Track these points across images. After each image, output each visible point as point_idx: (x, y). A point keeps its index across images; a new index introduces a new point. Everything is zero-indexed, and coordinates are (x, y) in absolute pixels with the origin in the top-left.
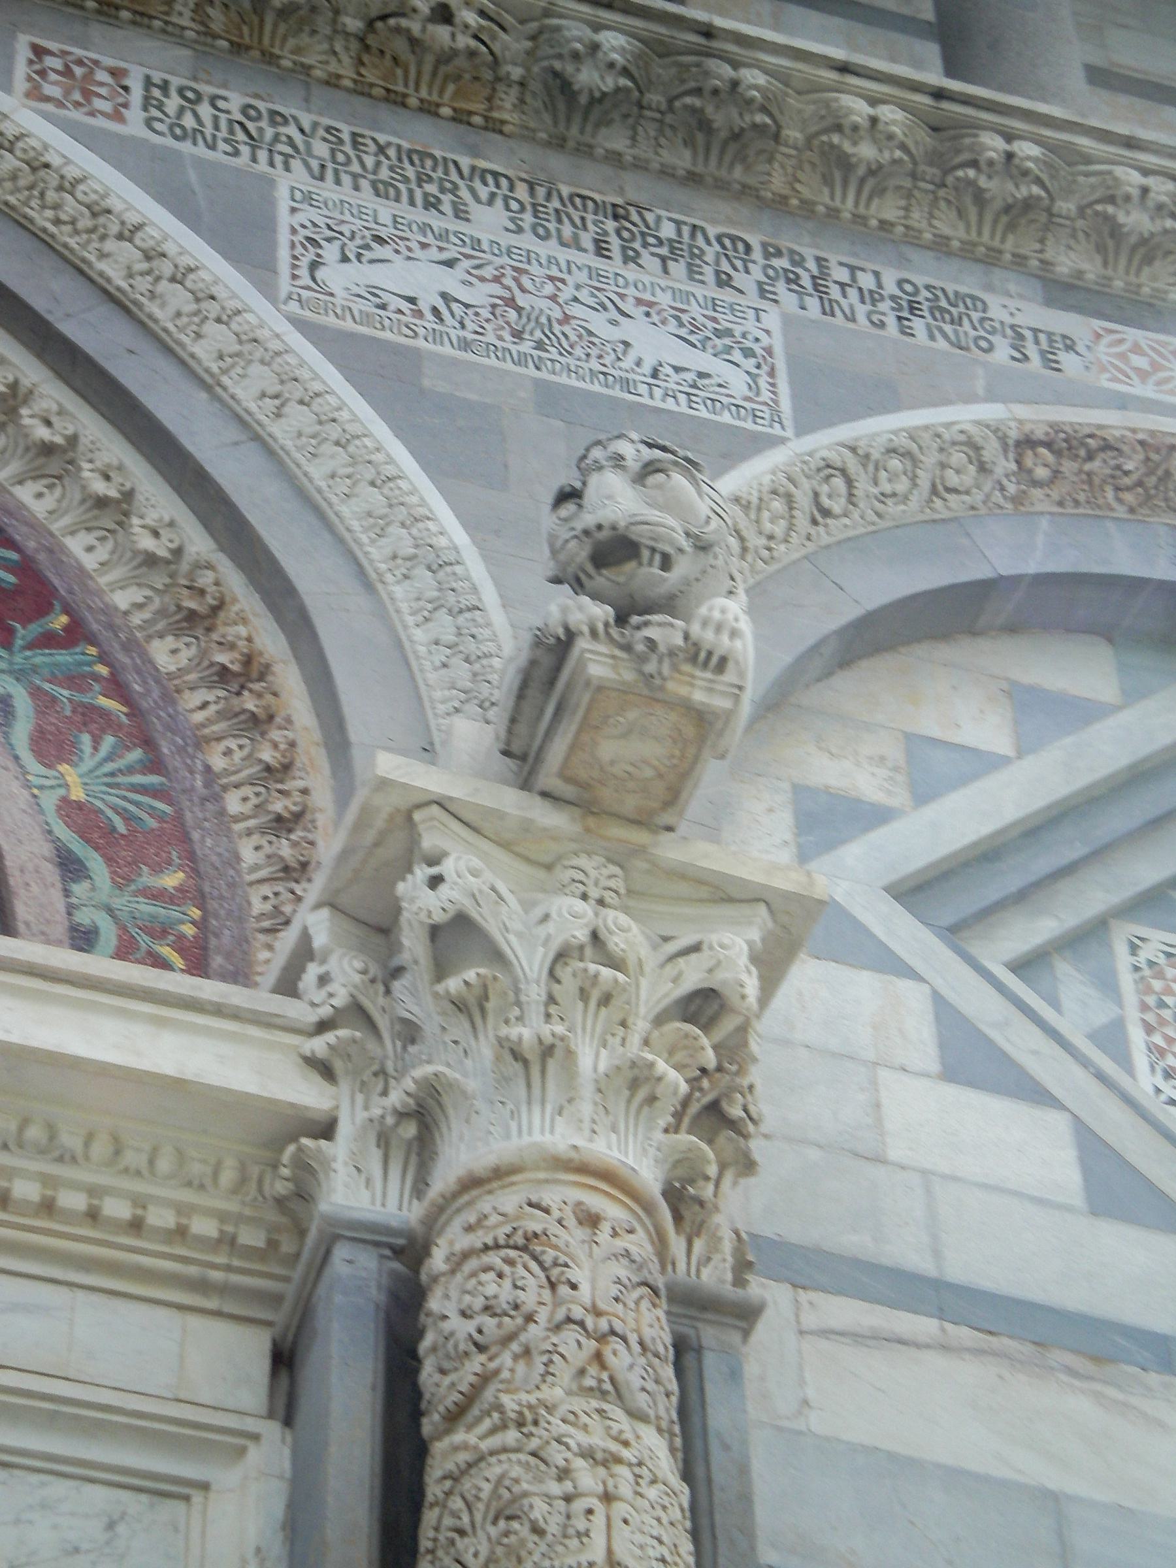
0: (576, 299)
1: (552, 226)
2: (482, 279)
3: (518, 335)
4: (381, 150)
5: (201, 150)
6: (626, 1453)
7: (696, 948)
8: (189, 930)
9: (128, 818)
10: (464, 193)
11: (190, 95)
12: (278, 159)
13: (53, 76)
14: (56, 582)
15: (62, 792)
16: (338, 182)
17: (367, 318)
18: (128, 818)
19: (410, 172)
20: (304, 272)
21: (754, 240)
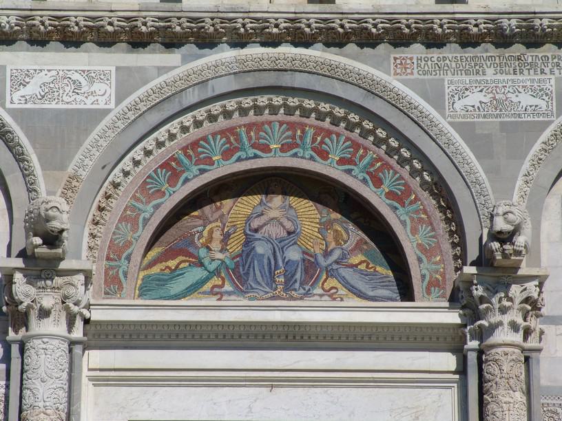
0: (509, 92)
1: (504, 69)
2: (488, 93)
3: (496, 109)
4: (467, 59)
5: (430, 77)
6: (512, 401)
7: (525, 289)
8: (442, 270)
9: (429, 245)
10: (485, 66)
11: (426, 59)
12: (445, 72)
13: (399, 66)
14: (412, 186)
16: (457, 74)
17: (464, 116)
18: (429, 245)
19: (473, 65)
20: (451, 107)
21: (549, 55)
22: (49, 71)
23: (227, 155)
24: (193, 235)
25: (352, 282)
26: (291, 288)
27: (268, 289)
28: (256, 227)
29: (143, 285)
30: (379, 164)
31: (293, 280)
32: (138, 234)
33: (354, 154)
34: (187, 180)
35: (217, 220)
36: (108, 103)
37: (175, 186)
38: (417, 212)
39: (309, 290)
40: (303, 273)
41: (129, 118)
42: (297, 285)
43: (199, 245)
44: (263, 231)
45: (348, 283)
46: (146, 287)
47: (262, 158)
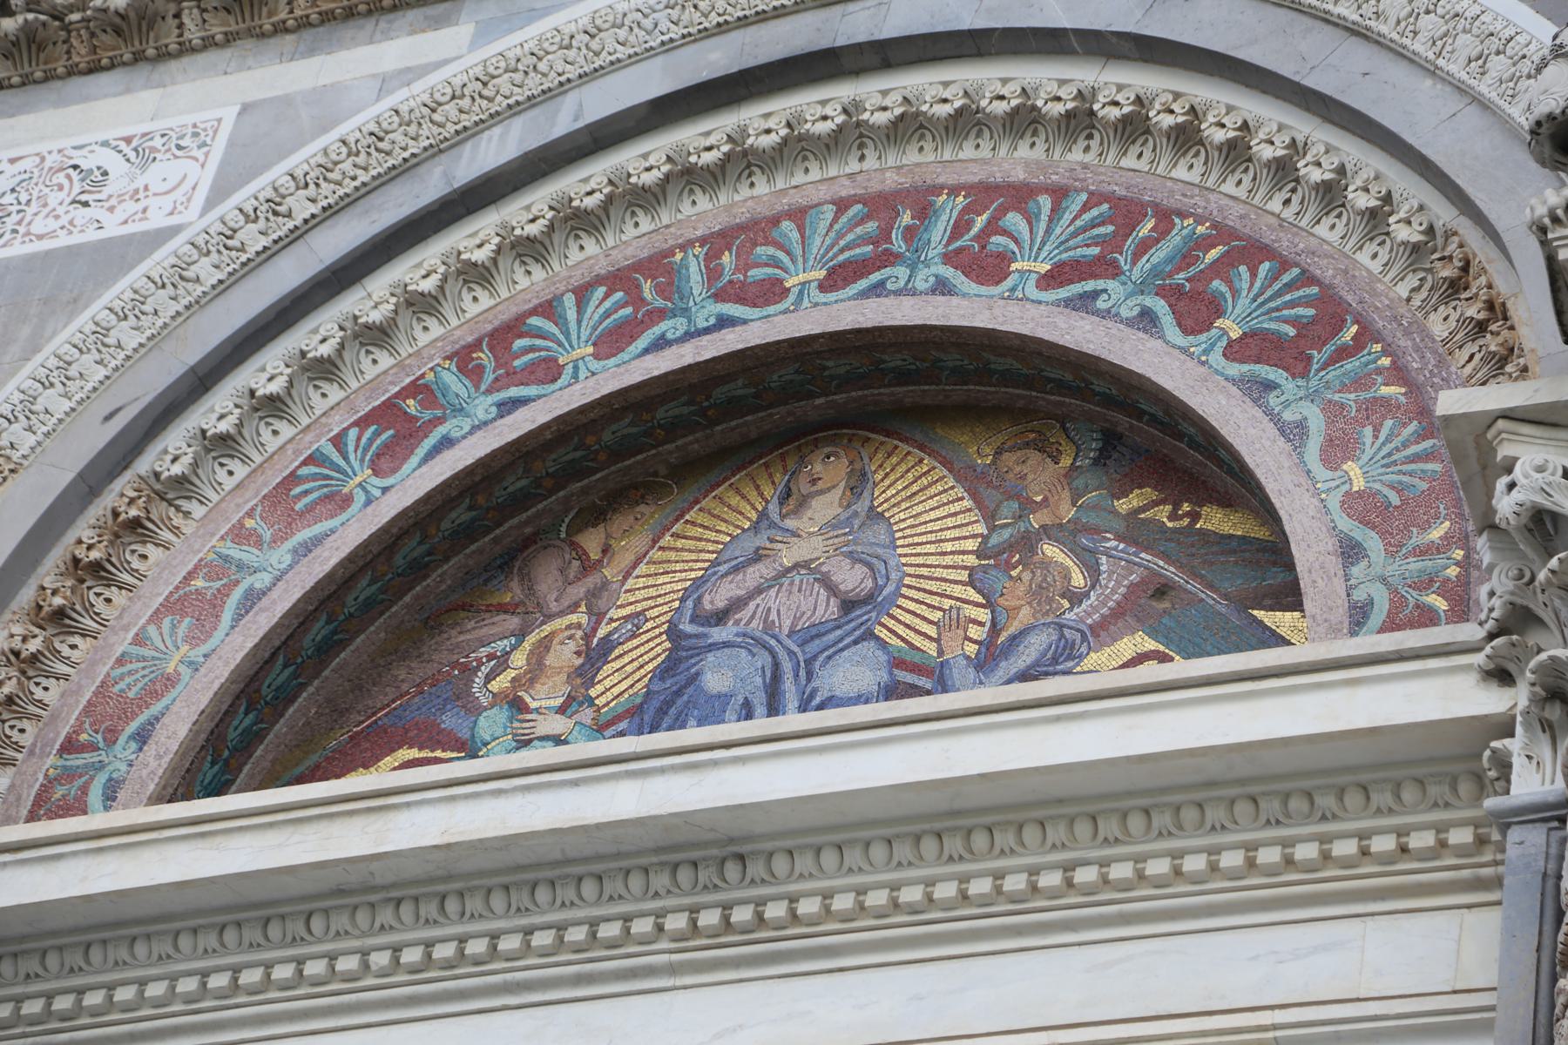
9: (1399, 488)
14: (1349, 298)
15: (1347, 487)
22: (12, 161)
23: (611, 342)
24: (469, 671)
28: (721, 604)
30: (1214, 253)
32: (205, 648)
33: (1113, 244)
34: (447, 442)
35: (573, 608)
36: (180, 208)
37: (394, 470)
38: (1359, 382)
41: (242, 249)
43: (484, 702)
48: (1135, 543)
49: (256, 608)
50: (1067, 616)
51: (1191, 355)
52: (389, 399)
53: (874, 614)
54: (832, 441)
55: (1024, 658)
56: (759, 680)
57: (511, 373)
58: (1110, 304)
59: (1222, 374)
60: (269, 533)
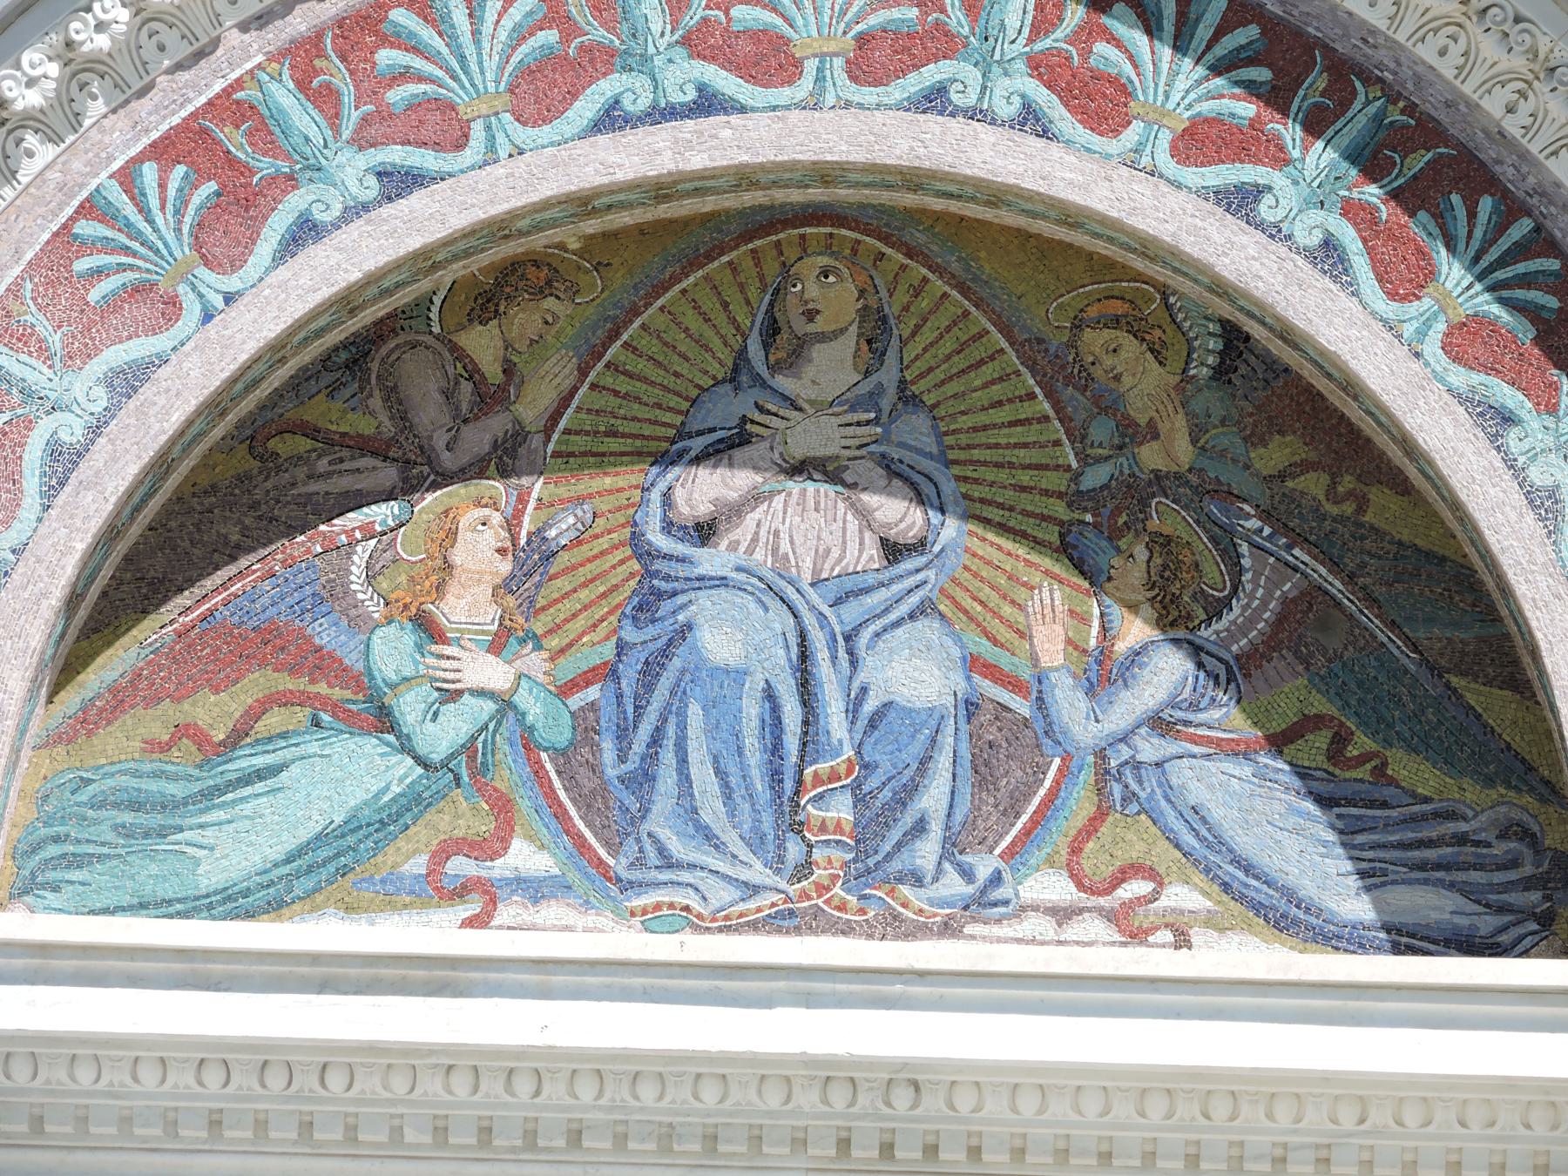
25: (1245, 843)
26: (896, 865)
27: (757, 872)
28: (704, 510)
29: (44, 832)
31: (908, 820)
34: (306, 232)
37: (236, 264)
39: (996, 879)
40: (965, 770)
42: (927, 852)
43: (376, 609)
44: (743, 532)
45: (1218, 842)
46: (56, 839)
47: (743, 109)
48: (1282, 528)
49: (73, 480)
50: (1203, 633)
51: (1399, 336)
52: (194, 115)
53: (930, 574)
54: (828, 245)
55: (1150, 690)
56: (782, 652)
57: (384, 115)
58: (1281, 213)
59: (1442, 381)
60: (57, 337)
